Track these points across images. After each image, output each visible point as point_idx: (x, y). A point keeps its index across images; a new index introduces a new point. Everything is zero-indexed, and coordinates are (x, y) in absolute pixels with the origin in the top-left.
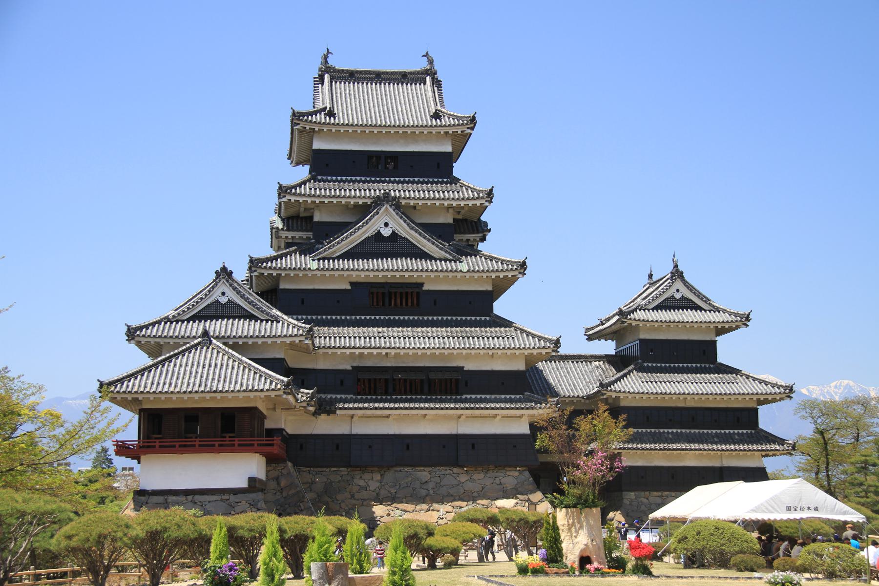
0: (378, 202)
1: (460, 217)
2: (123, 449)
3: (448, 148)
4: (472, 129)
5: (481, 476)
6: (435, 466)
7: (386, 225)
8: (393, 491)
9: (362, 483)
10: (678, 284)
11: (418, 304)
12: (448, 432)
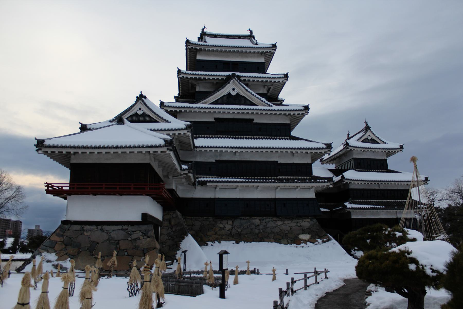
0: (229, 79)
3: (262, 60)
4: (275, 50)
5: (289, 222)
6: (263, 216)
7: (234, 89)
8: (239, 230)
9: (221, 226)
12: (270, 197)
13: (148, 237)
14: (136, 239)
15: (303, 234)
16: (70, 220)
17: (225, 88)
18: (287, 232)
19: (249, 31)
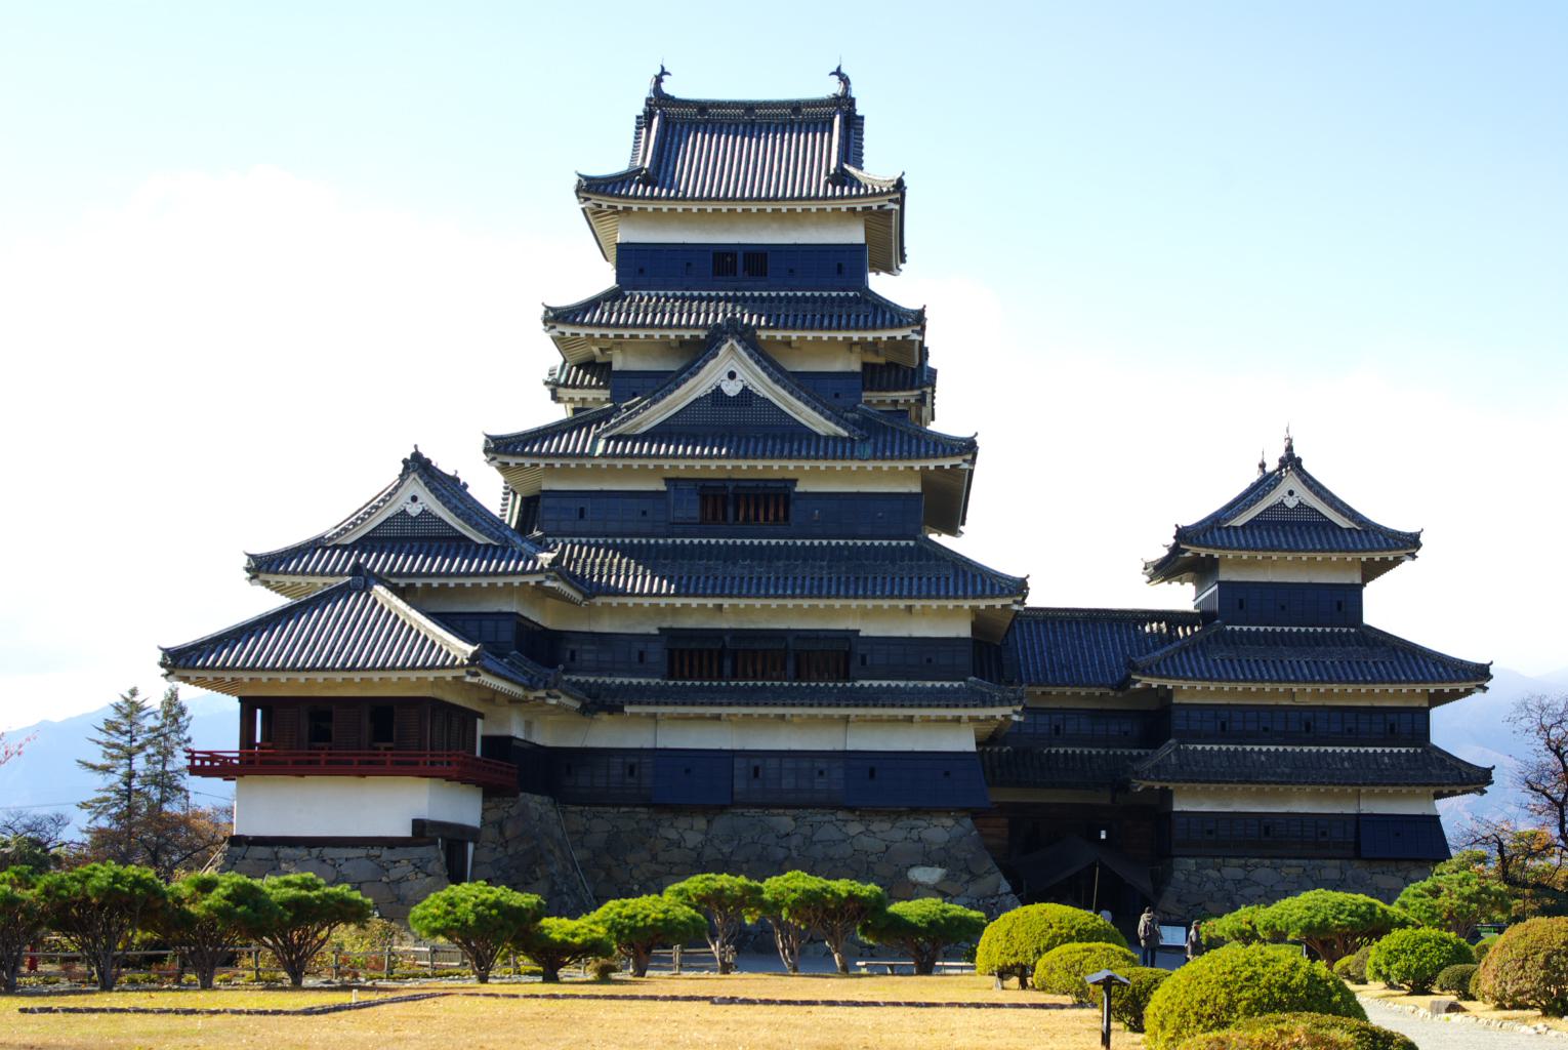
1: (881, 360)
2: (210, 766)
3: (855, 235)
4: (901, 202)
5: (886, 826)
6: (805, 807)
7: (732, 375)
8: (726, 849)
9: (673, 835)
10: (1291, 482)
11: (786, 517)
13: (429, 875)
14: (398, 881)
15: (923, 865)
16: (246, 834)
17: (703, 373)
18: (873, 858)
19: (836, 78)
